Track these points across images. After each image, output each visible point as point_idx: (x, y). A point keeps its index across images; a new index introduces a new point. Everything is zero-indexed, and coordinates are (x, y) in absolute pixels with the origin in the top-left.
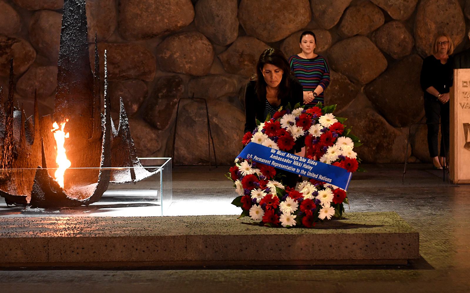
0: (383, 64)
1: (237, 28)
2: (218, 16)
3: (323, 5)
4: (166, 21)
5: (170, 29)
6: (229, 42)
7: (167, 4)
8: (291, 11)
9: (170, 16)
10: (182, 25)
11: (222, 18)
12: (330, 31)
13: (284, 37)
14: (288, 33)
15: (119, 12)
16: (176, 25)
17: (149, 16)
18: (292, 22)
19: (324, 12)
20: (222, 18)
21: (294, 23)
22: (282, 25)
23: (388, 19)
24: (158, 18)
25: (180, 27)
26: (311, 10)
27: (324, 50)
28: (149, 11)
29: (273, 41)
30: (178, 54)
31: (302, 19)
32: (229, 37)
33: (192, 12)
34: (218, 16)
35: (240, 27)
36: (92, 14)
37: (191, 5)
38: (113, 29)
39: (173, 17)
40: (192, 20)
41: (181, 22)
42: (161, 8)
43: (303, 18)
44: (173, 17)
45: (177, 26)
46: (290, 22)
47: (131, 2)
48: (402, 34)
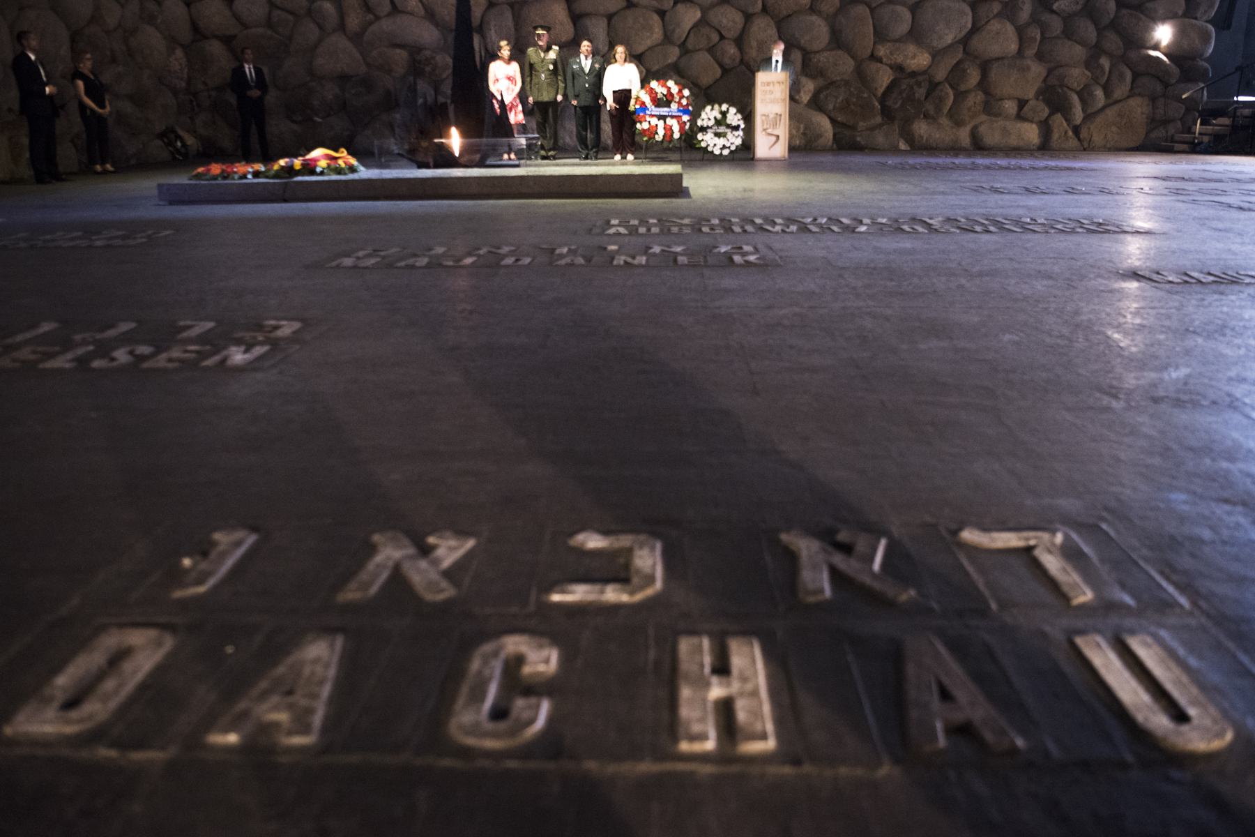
0: (719, 72)
12: (679, 46)
15: (516, 30)
19: (674, 31)
23: (722, 37)
48: (732, 50)
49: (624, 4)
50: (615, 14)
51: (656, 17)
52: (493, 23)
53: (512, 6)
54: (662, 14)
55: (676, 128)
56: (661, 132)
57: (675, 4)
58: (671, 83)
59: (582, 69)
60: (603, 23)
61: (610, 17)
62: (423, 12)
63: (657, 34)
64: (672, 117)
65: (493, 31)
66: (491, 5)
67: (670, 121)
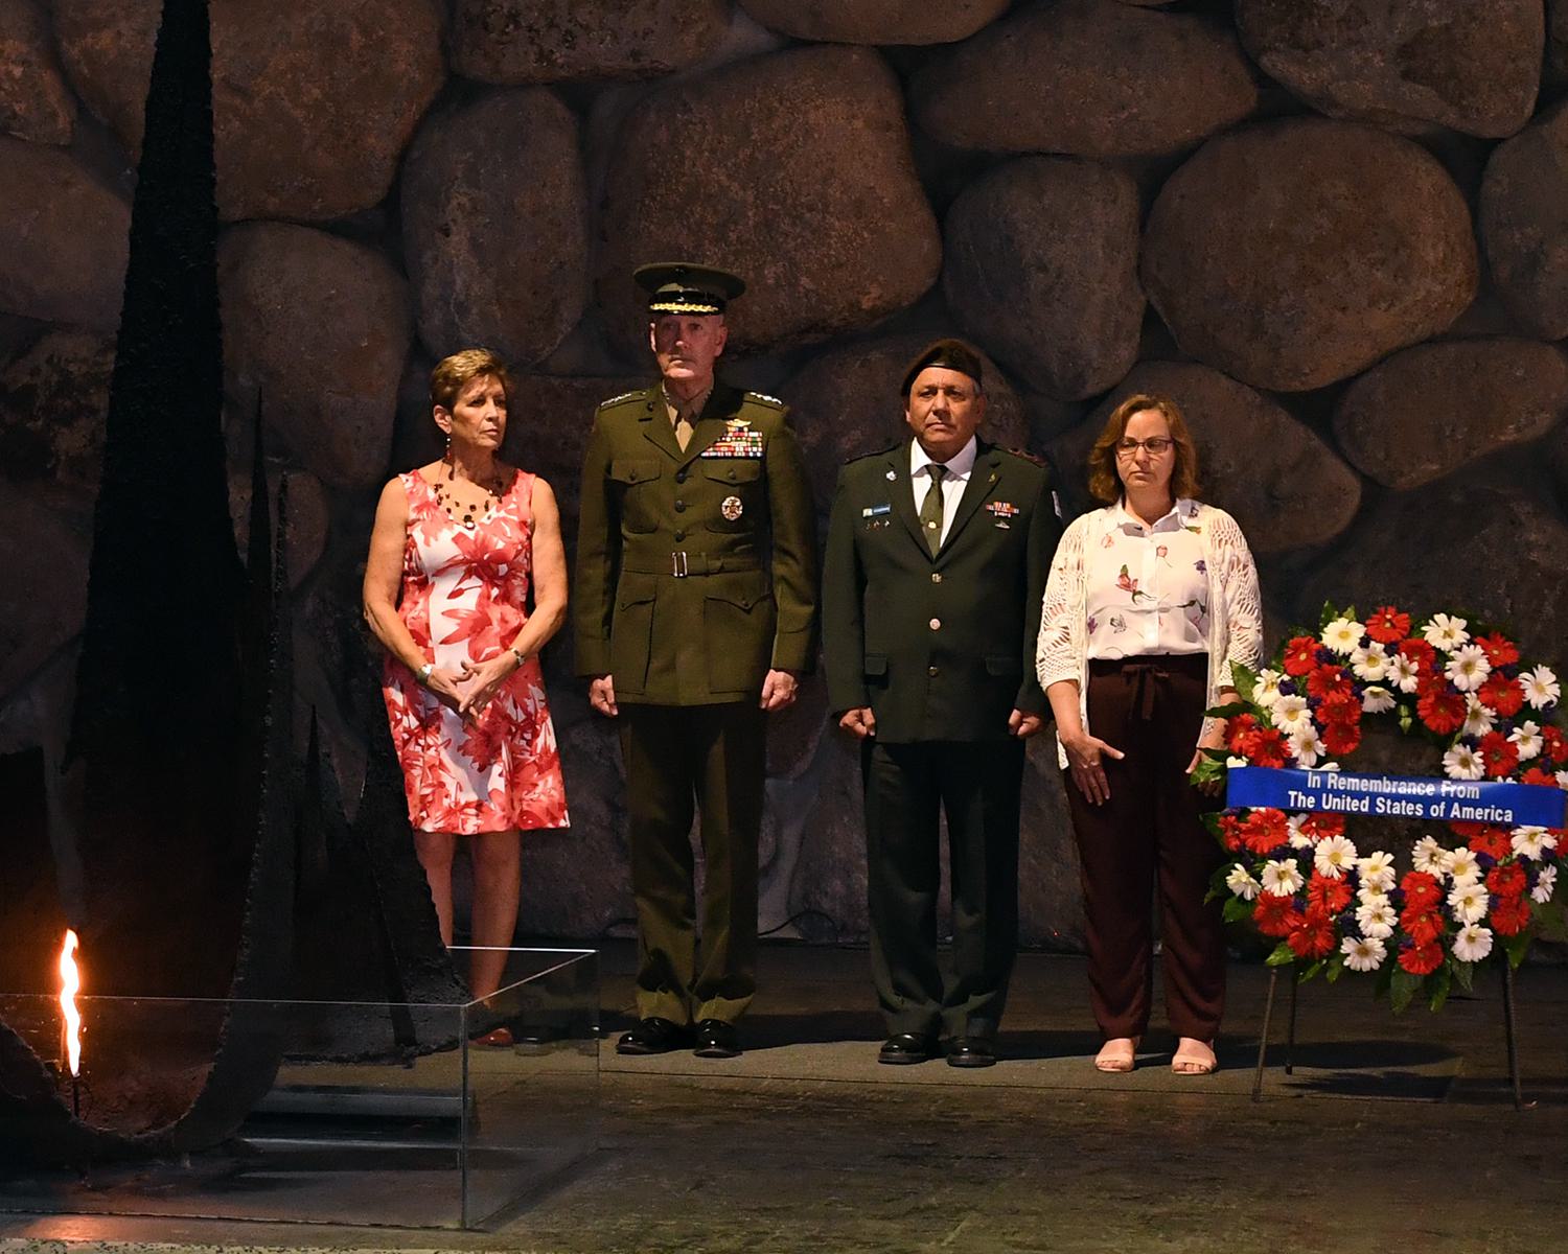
1: (1134, 321)
2: (1043, 268)
3: (1529, 230)
4: (804, 280)
5: (824, 321)
6: (1092, 388)
7: (811, 209)
8: (1377, 254)
9: (826, 261)
10: (878, 303)
11: (1059, 276)
13: (1351, 371)
14: (1365, 353)
16: (854, 306)
17: (731, 258)
18: (1384, 305)
20: (1059, 276)
21: (1393, 311)
22: (1339, 315)
24: (770, 273)
25: (873, 313)
26: (1481, 249)
27: (1529, 434)
28: (733, 236)
29: (1296, 386)
30: (856, 434)
31: (1429, 292)
32: (1095, 365)
33: (928, 245)
34: (1043, 268)
35: (1150, 318)
36: (476, 247)
37: (923, 215)
38: (569, 313)
39: (840, 266)
40: (931, 282)
41: (875, 291)
42: (784, 227)
43: (1438, 288)
44: (840, 266)
45: (860, 309)
46: (1372, 303)
47: (654, 199)
49: (1247, 99)
50: (1185, 155)
51: (1428, 177)
52: (460, 198)
53: (578, 94)
54: (1466, 158)
55: (1470, 899)
56: (1376, 918)
57: (1547, 103)
58: (1445, 631)
59: (909, 526)
60: (1109, 211)
61: (1154, 175)
62: (62, 122)
63: (1436, 282)
64: (1450, 835)
65: (457, 245)
66: (457, 92)
67: (1428, 858)
